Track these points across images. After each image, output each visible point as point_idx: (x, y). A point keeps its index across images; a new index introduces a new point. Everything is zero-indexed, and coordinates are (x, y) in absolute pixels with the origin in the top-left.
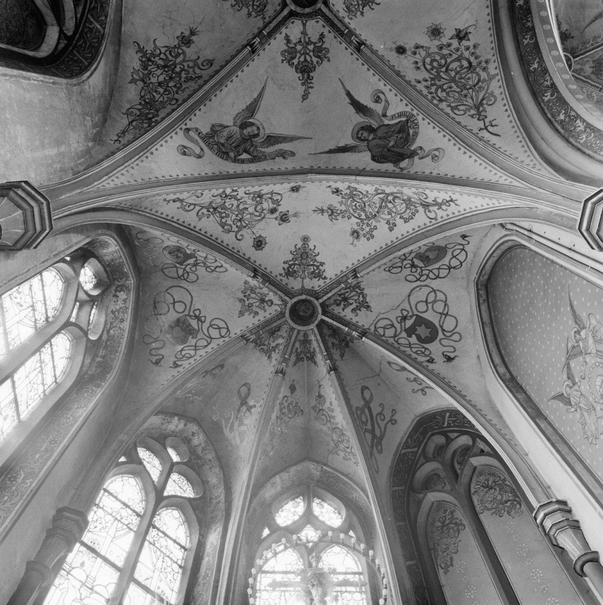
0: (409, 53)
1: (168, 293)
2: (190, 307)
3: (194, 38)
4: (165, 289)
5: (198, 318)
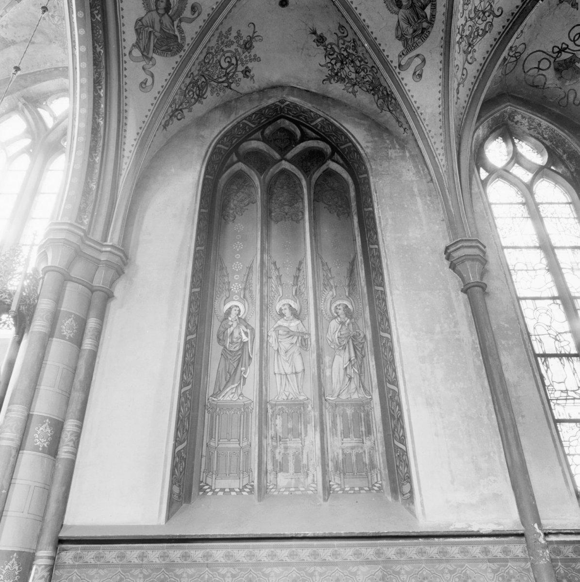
1: (528, 71)
2: (548, 54)
3: (319, 33)
4: (523, 74)
5: (562, 50)
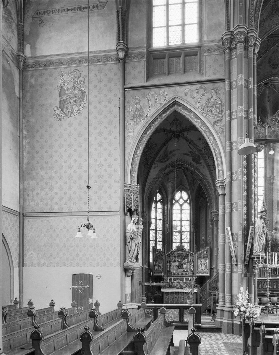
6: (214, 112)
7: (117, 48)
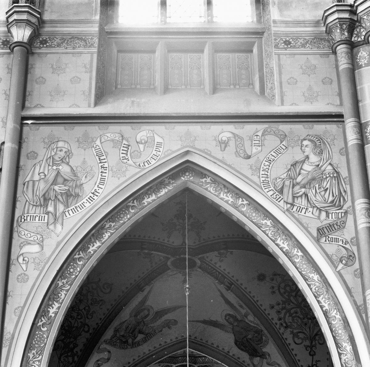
0: (268, 279)
6: (317, 199)
7: (7, 18)
